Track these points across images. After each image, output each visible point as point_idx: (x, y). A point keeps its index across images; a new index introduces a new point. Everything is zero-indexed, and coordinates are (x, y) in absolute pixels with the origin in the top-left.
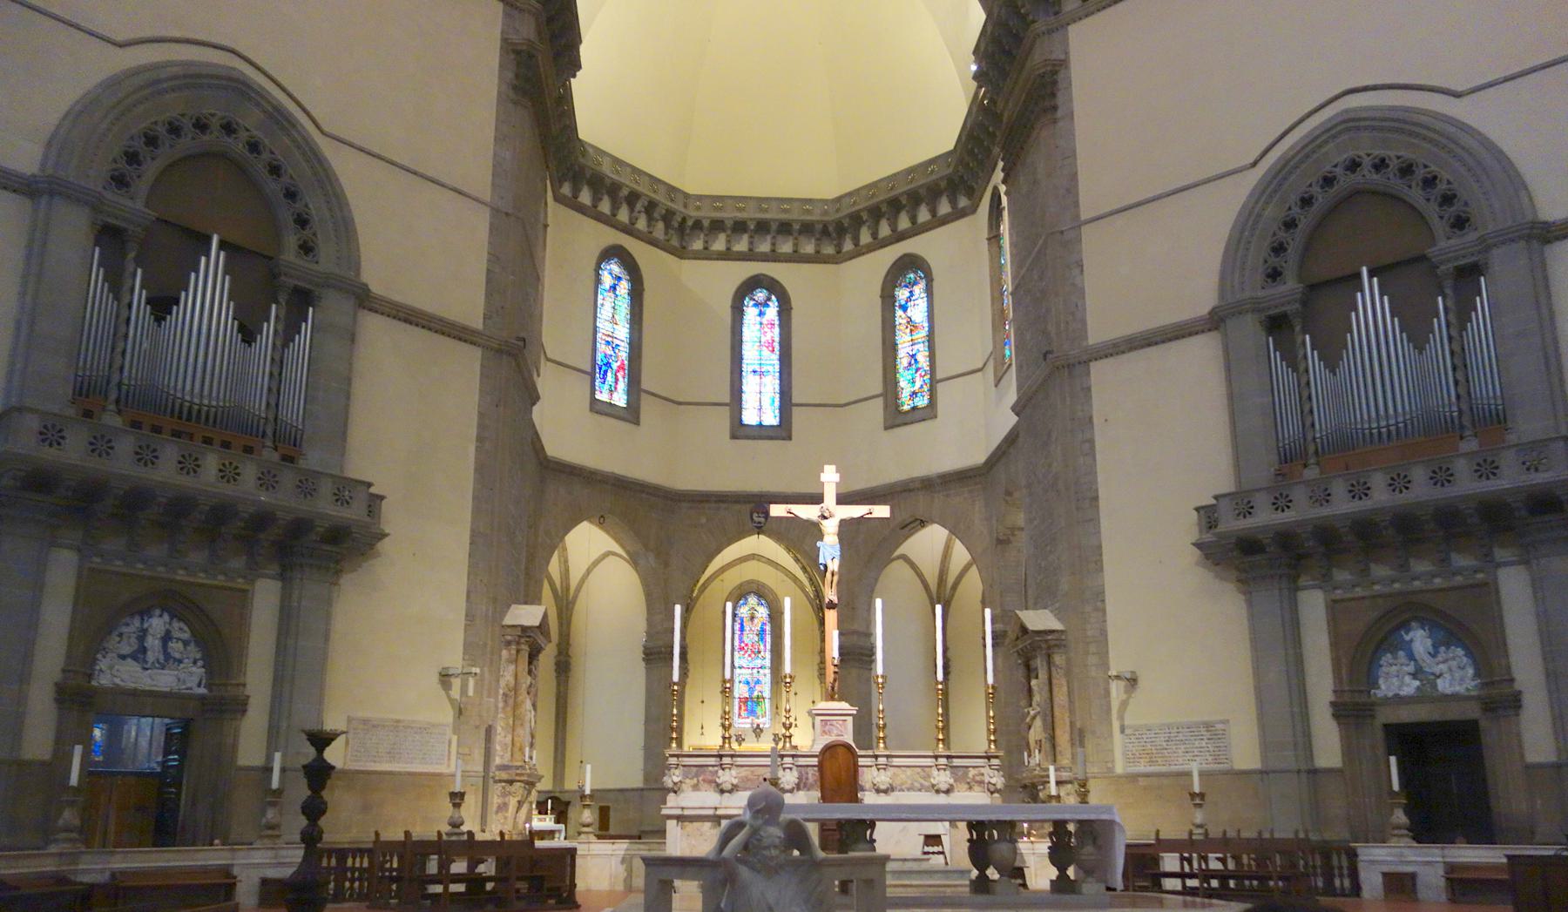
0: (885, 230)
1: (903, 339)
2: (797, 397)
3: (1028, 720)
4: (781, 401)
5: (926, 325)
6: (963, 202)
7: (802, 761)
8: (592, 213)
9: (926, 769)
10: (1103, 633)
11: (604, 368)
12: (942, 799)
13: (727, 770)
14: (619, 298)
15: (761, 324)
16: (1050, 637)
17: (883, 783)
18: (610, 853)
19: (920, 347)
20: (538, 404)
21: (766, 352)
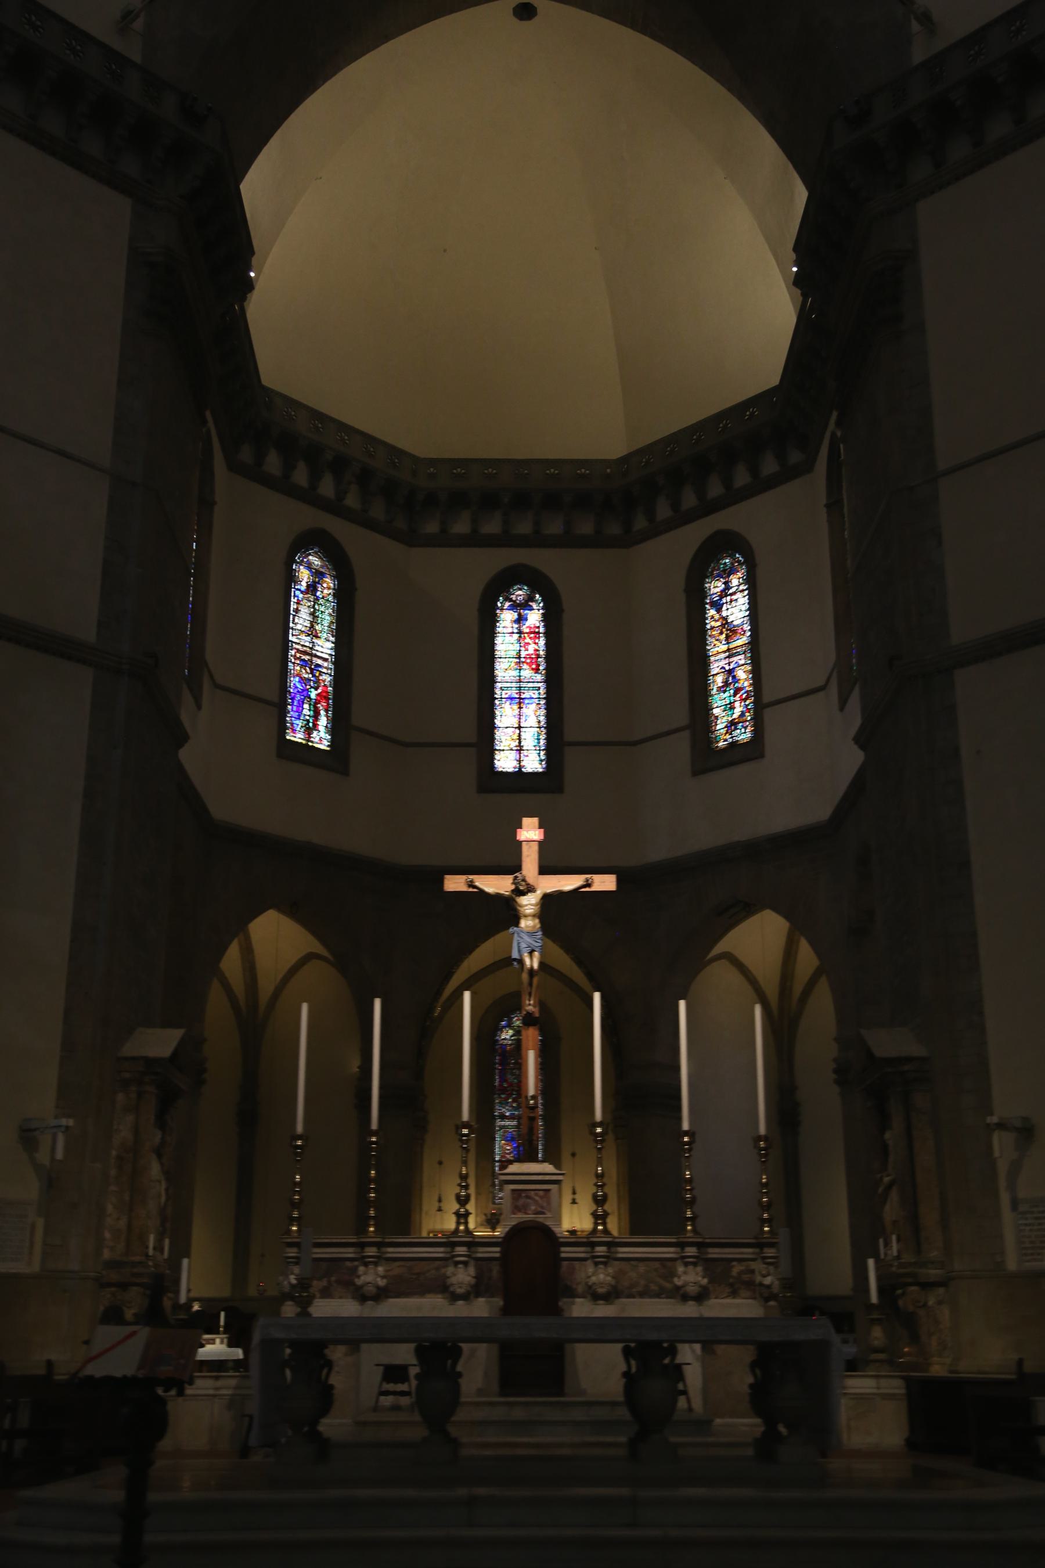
0: (689, 499)
1: (717, 647)
2: (570, 734)
3: (880, 1190)
5: (747, 627)
6: (795, 457)
7: (482, 1252)
8: (283, 486)
9: (669, 1264)
11: (298, 697)
12: (689, 1310)
14: (321, 601)
15: (520, 632)
18: (211, 1392)
19: (741, 659)
20: (187, 746)
21: (527, 673)
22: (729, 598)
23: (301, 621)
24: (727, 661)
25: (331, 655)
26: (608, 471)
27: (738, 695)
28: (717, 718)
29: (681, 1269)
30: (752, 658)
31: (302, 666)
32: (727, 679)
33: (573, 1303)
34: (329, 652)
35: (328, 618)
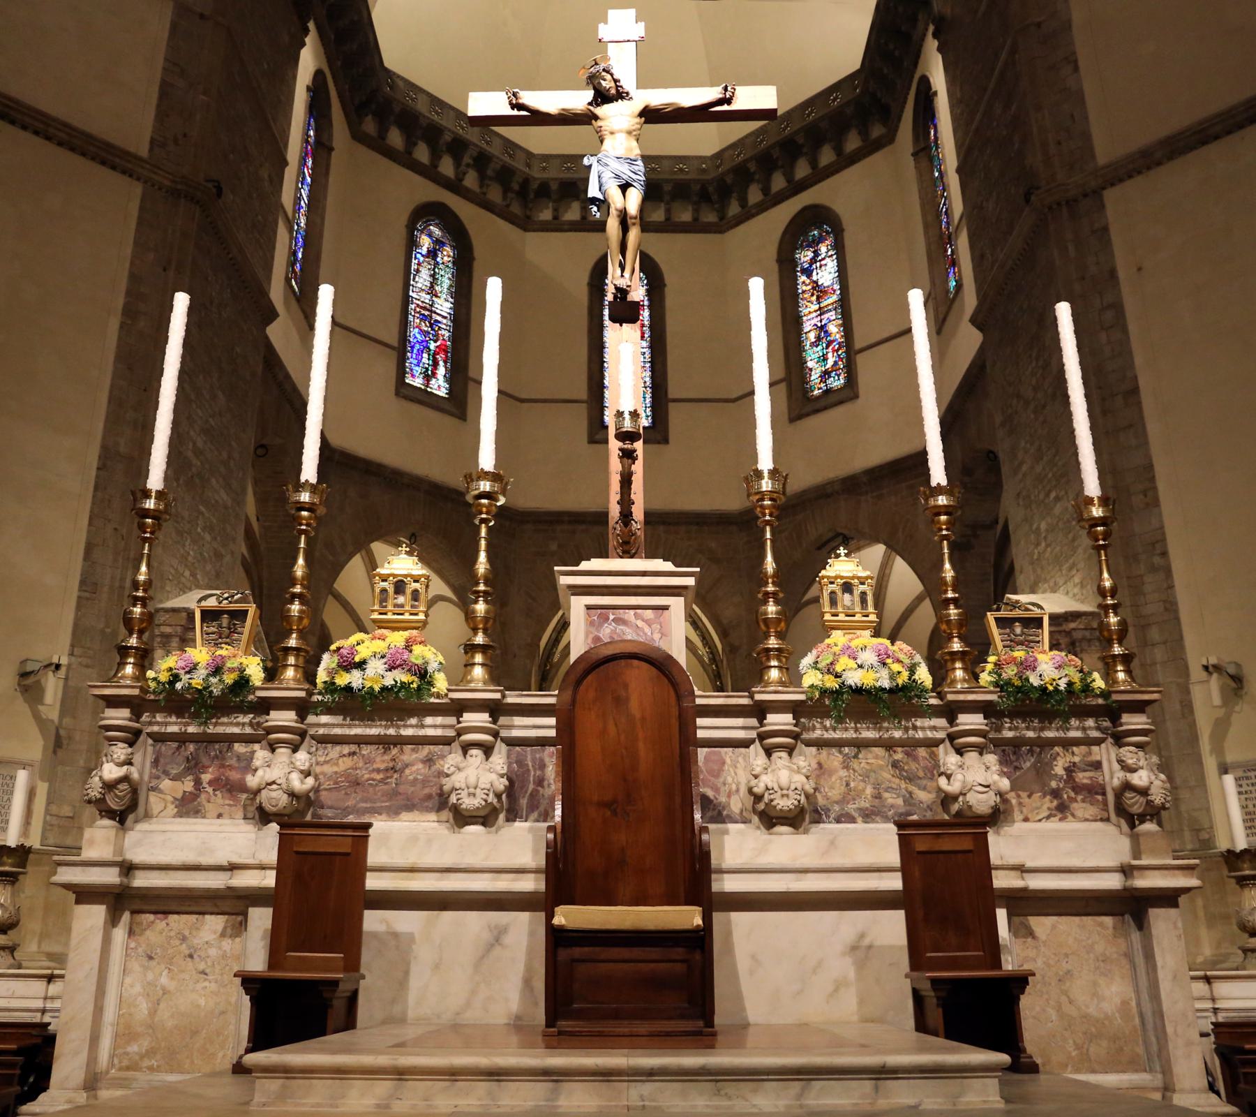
4: (652, 398)
5: (837, 287)
6: (877, 131)
7: (523, 727)
10: (1171, 607)
11: (417, 346)
13: (283, 752)
14: (441, 266)
16: (1072, 625)
17: (784, 791)
19: (832, 315)
22: (818, 264)
23: (421, 280)
24: (819, 318)
25: (449, 314)
26: (704, 166)
27: (831, 347)
28: (811, 370)
29: (950, 759)
30: (842, 313)
31: (421, 320)
32: (819, 335)
33: (726, 832)
34: (448, 311)
35: (447, 281)
